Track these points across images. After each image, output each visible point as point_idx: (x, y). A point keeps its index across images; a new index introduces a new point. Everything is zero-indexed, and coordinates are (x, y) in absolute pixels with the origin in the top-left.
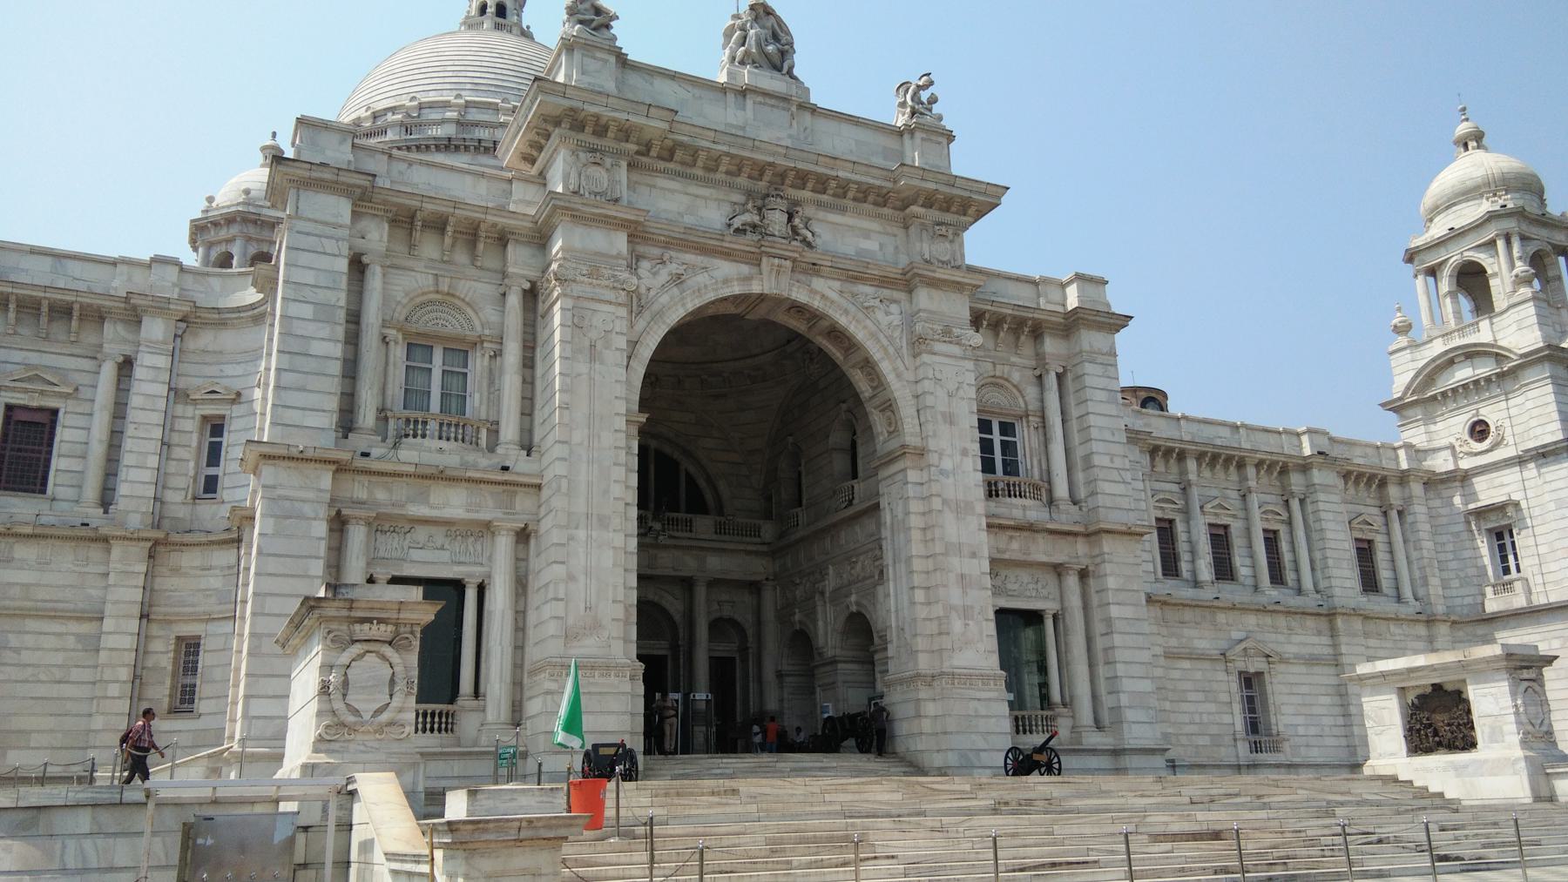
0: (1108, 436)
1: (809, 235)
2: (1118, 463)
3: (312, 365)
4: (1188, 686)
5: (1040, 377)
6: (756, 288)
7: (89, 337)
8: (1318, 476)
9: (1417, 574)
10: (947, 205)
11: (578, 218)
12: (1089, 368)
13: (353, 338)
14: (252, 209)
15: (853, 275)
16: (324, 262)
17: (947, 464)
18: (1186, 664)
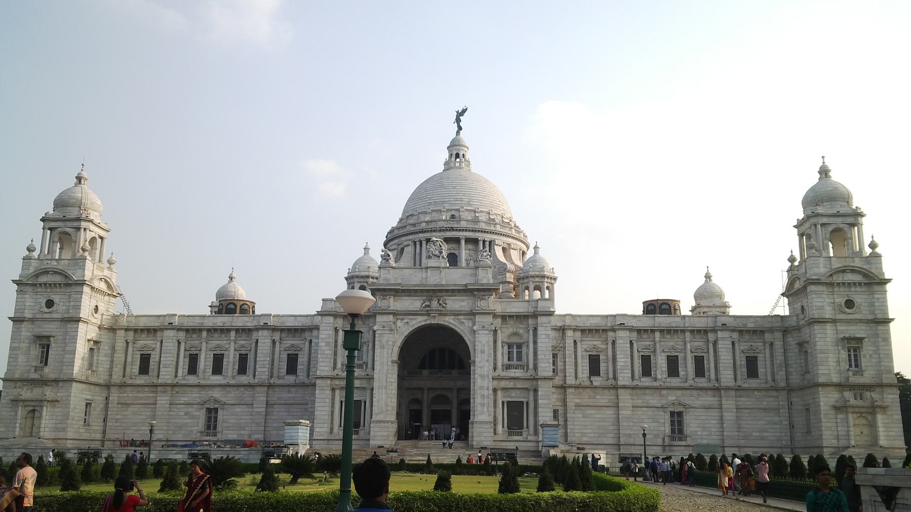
0: (545, 350)
1: (444, 305)
2: (547, 357)
3: (323, 356)
5: (529, 330)
6: (428, 322)
7: (303, 335)
8: (720, 334)
9: (775, 370)
10: (484, 290)
11: (380, 314)
12: (539, 328)
13: (336, 346)
14: (357, 274)
15: (456, 314)
16: (328, 332)
17: (480, 365)
18: (645, 409)
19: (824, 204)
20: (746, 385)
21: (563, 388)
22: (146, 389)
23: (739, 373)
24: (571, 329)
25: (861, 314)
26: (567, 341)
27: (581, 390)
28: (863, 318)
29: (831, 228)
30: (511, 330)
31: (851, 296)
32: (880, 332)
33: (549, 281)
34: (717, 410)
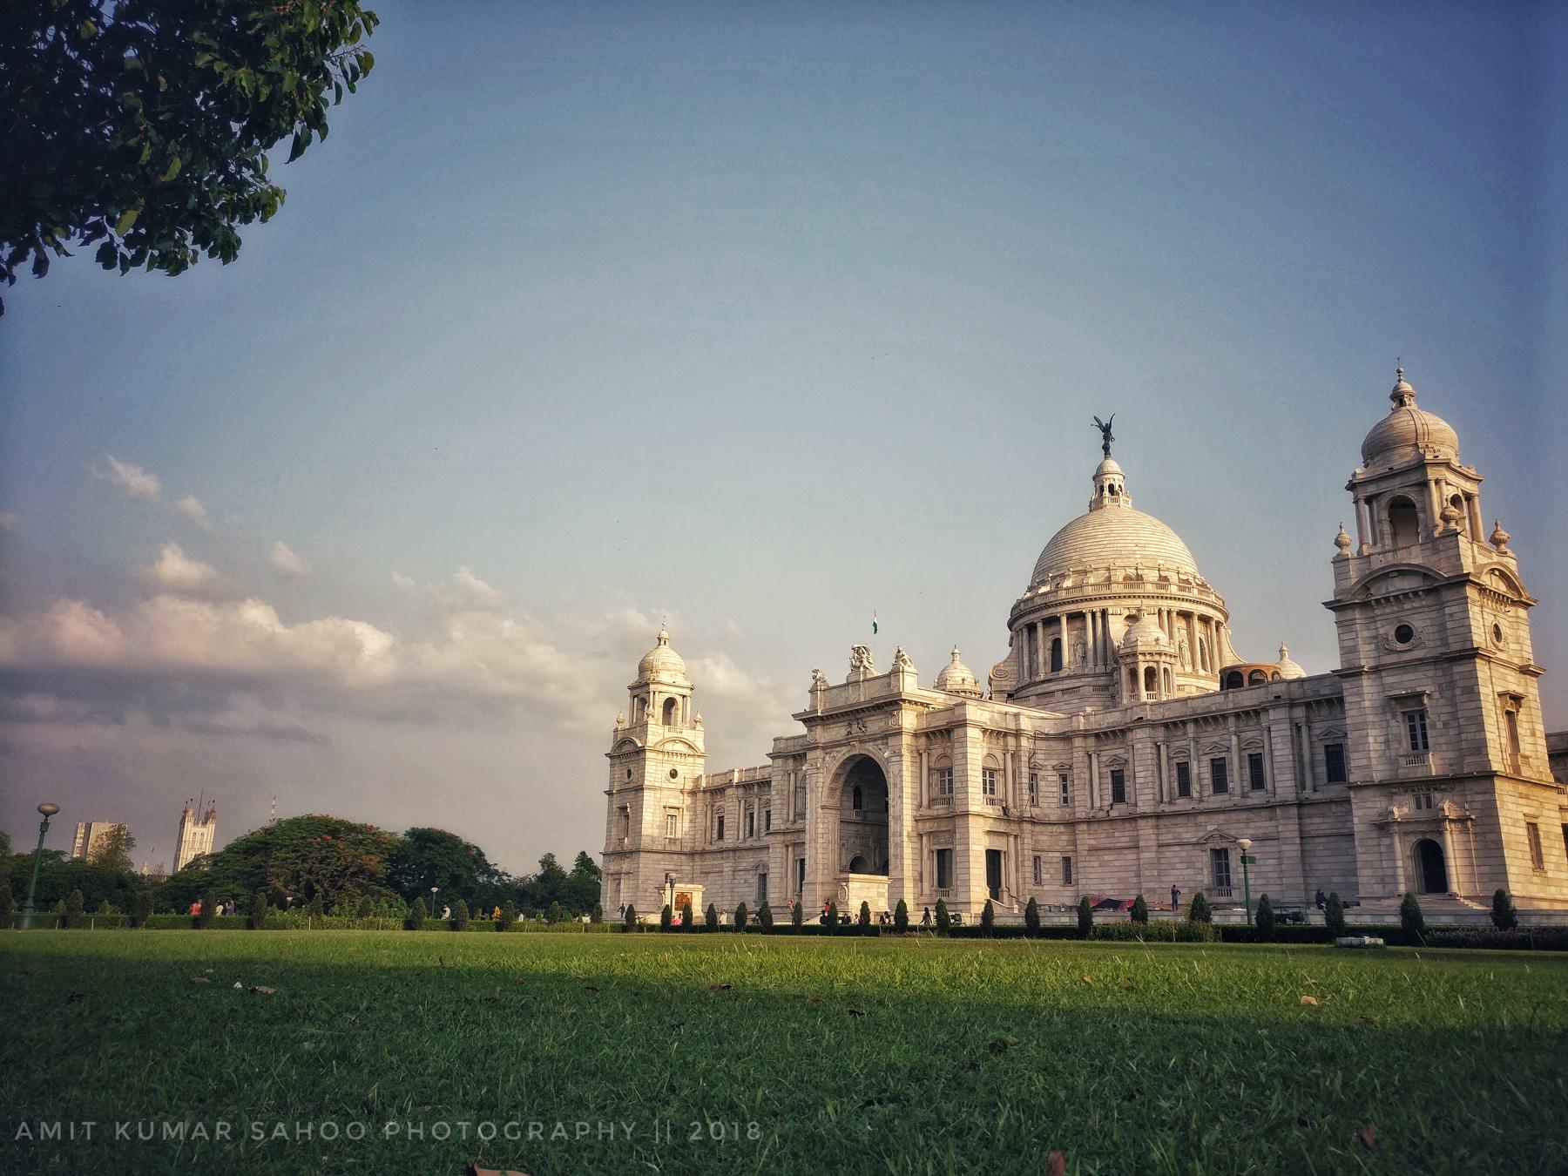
4: (1177, 860)
8: (1273, 714)
11: (810, 749)
18: (1177, 848)
19: (1376, 459)
20: (1318, 796)
21: (1071, 824)
22: (719, 856)
23: (1308, 776)
24: (1078, 736)
25: (1424, 648)
26: (1075, 754)
27: (1095, 827)
28: (1428, 655)
29: (1384, 501)
30: (940, 751)
31: (1404, 619)
32: (1457, 677)
33: (1148, 657)
34: (1275, 842)
